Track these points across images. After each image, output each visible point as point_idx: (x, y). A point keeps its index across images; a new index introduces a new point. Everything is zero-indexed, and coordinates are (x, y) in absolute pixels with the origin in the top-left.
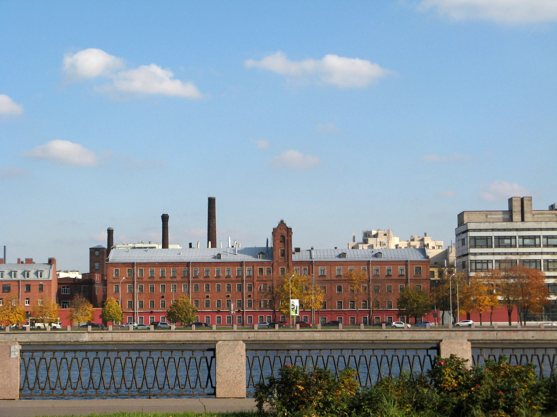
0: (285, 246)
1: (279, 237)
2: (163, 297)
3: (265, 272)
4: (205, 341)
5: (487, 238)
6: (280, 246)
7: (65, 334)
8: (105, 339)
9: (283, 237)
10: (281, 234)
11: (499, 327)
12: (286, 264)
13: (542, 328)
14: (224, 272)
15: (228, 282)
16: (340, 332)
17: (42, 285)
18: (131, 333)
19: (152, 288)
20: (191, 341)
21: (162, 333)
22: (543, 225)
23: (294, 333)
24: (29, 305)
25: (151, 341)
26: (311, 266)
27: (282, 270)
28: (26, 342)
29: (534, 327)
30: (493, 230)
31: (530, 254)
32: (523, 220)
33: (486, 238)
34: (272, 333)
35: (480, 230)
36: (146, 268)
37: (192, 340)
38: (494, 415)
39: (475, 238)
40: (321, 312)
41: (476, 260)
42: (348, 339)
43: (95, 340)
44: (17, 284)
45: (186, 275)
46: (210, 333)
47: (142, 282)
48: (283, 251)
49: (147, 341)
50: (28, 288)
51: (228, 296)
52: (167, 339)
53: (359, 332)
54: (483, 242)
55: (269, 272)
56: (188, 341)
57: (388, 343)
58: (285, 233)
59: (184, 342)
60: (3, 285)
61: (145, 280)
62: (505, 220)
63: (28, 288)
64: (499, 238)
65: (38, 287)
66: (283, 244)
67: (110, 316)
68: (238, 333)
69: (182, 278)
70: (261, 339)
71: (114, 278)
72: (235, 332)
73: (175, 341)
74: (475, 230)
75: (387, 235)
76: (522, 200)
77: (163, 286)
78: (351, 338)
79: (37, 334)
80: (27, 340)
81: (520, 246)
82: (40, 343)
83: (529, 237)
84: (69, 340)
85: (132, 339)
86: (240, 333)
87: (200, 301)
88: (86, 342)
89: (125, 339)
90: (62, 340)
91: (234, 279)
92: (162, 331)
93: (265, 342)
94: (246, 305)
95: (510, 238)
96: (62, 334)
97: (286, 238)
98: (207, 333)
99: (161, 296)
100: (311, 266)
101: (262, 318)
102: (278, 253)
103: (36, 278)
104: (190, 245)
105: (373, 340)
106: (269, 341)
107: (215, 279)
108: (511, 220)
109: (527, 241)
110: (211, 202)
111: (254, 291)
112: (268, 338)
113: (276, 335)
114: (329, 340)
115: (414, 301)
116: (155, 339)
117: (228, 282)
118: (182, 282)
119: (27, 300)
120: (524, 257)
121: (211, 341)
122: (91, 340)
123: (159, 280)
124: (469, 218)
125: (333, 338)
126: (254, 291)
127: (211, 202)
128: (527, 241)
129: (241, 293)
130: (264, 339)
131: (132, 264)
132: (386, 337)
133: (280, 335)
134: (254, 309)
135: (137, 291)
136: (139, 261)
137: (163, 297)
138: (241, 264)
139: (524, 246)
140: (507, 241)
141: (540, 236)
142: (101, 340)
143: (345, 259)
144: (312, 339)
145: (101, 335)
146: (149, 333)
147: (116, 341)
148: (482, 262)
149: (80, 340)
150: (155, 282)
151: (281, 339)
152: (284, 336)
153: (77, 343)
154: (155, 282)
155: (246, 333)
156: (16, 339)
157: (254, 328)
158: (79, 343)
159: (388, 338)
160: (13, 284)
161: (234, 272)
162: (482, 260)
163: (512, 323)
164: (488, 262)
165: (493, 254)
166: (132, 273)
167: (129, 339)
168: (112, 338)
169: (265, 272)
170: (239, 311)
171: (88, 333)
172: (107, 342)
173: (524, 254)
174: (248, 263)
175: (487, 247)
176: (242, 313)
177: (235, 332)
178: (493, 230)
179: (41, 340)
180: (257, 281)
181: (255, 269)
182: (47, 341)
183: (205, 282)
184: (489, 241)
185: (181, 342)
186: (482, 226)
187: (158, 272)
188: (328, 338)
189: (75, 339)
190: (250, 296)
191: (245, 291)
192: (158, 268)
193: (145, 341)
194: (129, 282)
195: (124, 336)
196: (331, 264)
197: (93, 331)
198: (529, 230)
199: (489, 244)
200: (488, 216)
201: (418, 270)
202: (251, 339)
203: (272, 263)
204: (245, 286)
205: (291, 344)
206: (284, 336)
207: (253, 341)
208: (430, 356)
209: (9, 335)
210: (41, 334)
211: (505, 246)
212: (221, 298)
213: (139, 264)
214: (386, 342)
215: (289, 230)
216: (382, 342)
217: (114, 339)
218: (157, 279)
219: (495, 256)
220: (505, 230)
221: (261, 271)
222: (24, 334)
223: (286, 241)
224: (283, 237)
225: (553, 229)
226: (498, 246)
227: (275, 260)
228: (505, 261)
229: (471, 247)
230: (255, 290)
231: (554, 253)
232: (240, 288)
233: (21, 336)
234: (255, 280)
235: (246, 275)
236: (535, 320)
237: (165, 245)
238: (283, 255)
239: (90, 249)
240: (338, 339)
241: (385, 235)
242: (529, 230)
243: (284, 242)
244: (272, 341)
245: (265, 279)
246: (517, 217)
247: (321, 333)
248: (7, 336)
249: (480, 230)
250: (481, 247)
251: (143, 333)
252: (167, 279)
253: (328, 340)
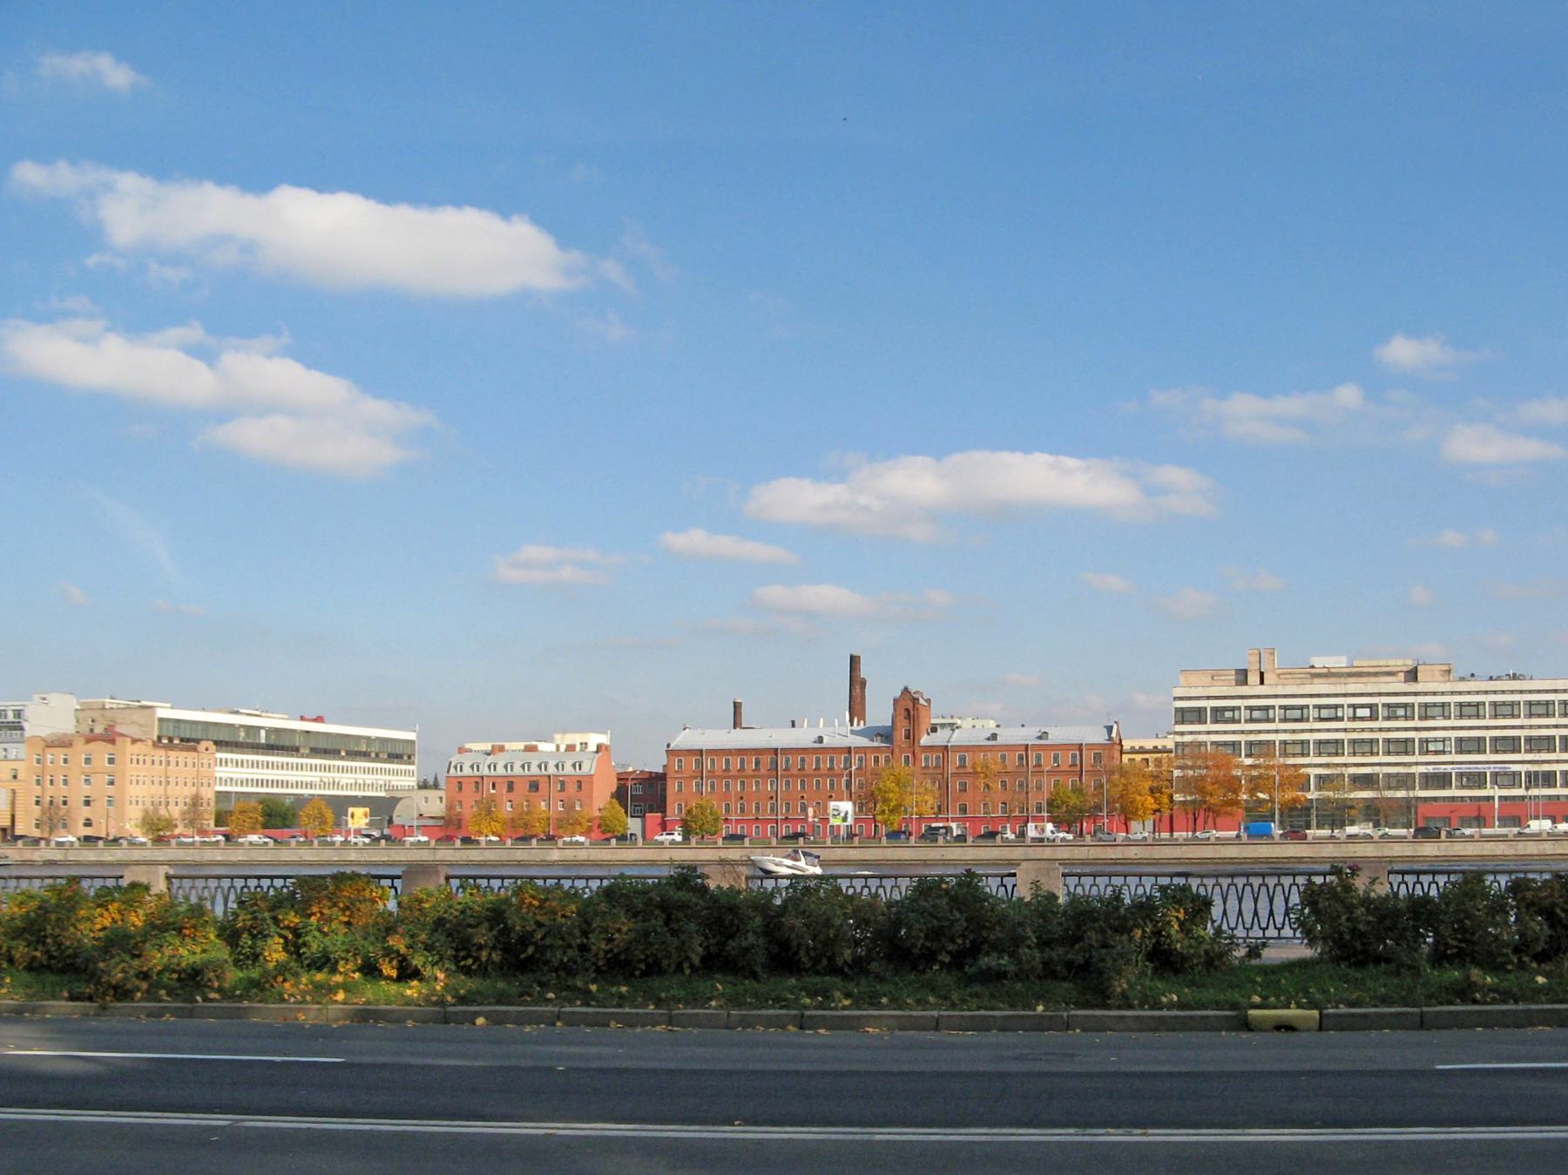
2: (742, 798)
9: (907, 710)
12: (911, 750)
19: (727, 785)
30: (1208, 698)
32: (1262, 682)
35: (1190, 698)
47: (714, 777)
52: (658, 859)
54: (1195, 716)
55: (887, 760)
58: (910, 706)
61: (717, 774)
64: (1215, 710)
77: (743, 783)
78: (896, 858)
81: (1246, 721)
83: (1259, 708)
85: (614, 858)
95: (1233, 709)
97: (912, 713)
102: (900, 734)
104: (793, 722)
107: (812, 772)
108: (1245, 682)
109: (1256, 714)
110: (854, 661)
115: (1063, 802)
128: (1256, 714)
137: (742, 798)
139: (1252, 720)
140: (1228, 714)
144: (846, 858)
165: (1208, 733)
166: (699, 763)
167: (609, 858)
173: (1251, 732)
174: (859, 749)
178: (1208, 698)
186: (1193, 693)
187: (736, 762)
201: (1098, 757)
208: (1251, 885)
211: (1226, 721)
212: (821, 798)
213: (710, 752)
221: (877, 760)
224: (907, 710)
226: (1216, 721)
229: (1176, 723)
238: (908, 737)
249: (1190, 698)
250: (1192, 723)
252: (746, 773)
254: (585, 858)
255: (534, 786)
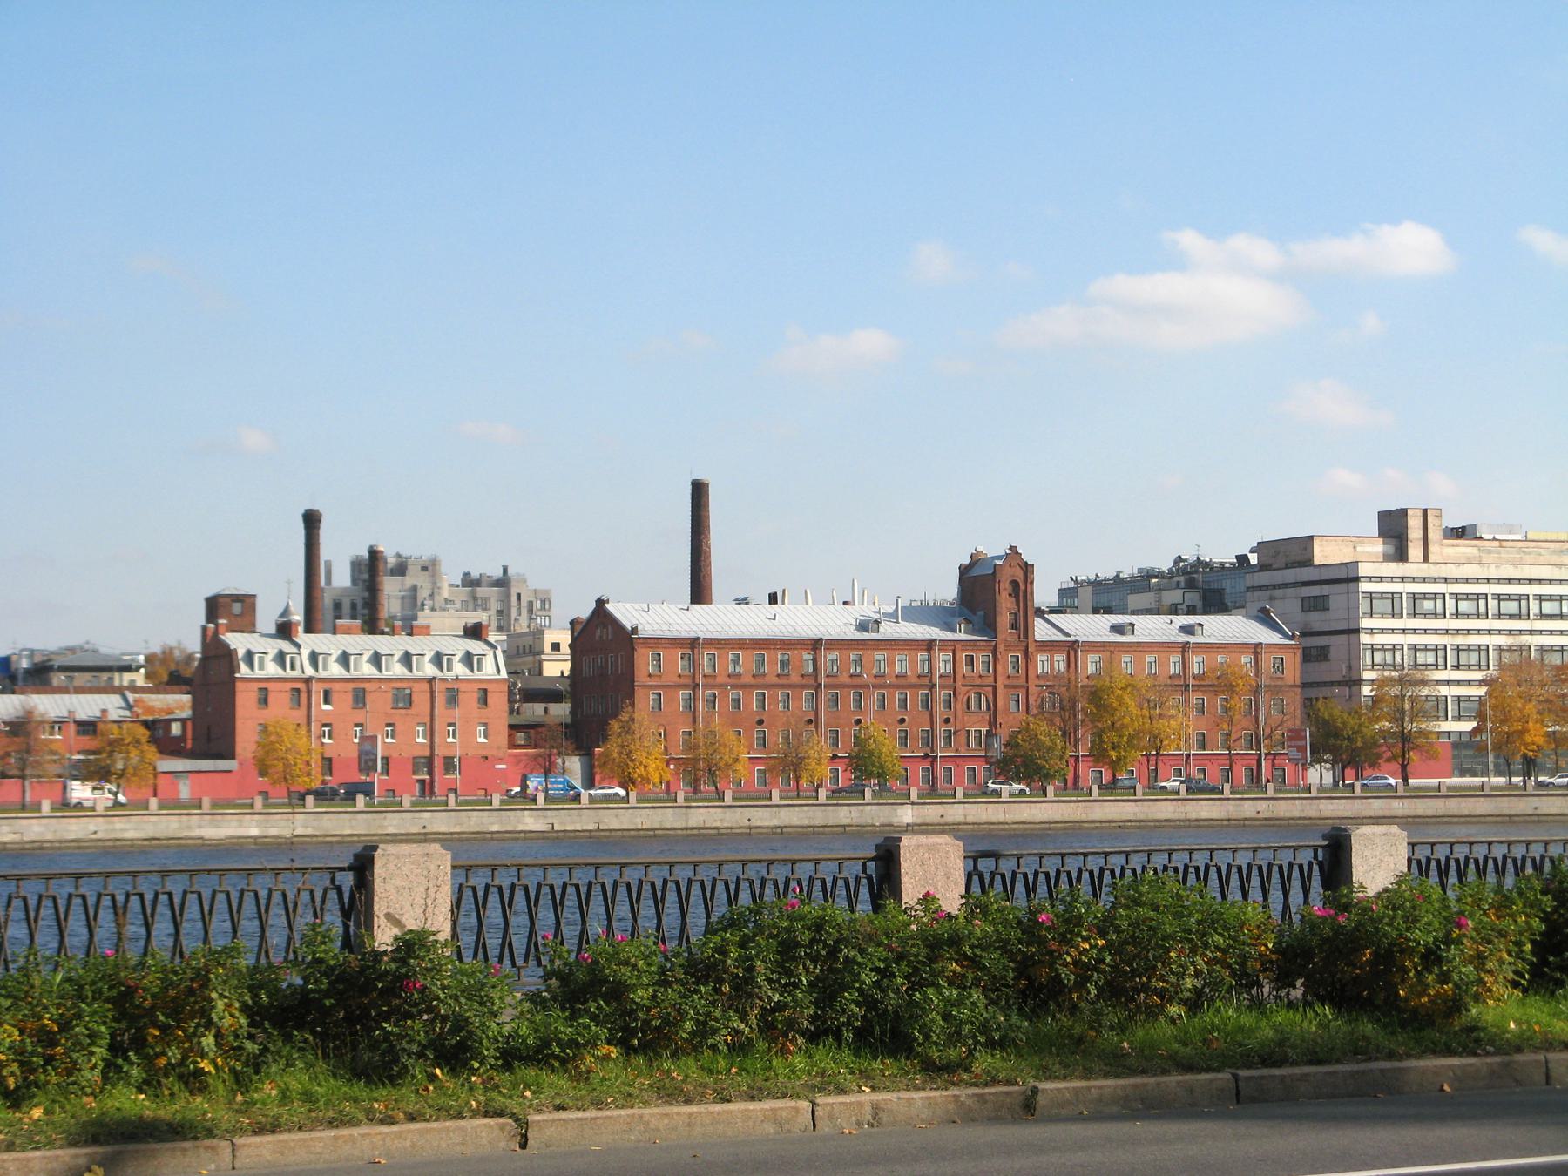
0: (1018, 604)
1: (1007, 585)
2: (761, 722)
3: (979, 667)
4: (1166, 820)
5: (1392, 597)
6: (1009, 606)
7: (861, 808)
8: (949, 819)
10: (1013, 576)
11: (1449, 788)
13: (1444, 792)
14: (892, 663)
15: (903, 687)
16: (1443, 800)
17: (485, 691)
18: (1005, 805)
20: (1135, 821)
21: (1072, 804)
22: (1493, 572)
23: (1349, 801)
24: (454, 740)
25: (1050, 823)
26: (1072, 653)
27: (1014, 660)
28: (772, 828)
29: (1470, 788)
31: (1541, 632)
32: (1426, 559)
33: (1390, 596)
34: (1304, 801)
36: (723, 651)
37: (1138, 818)
38: (1254, 991)
39: (1371, 596)
40: (1085, 759)
41: (1372, 645)
42: (1460, 814)
43: (927, 821)
44: (426, 686)
45: (811, 669)
46: (1174, 803)
48: (1013, 617)
49: (1041, 823)
50: (360, 698)
51: (902, 721)
52: (1084, 817)
53: (1482, 799)
54: (1384, 606)
56: (1130, 821)
57: (1539, 822)
59: (1121, 824)
60: (393, 688)
61: (720, 680)
62: (1387, 558)
63: (360, 698)
64: (1414, 597)
65: (476, 695)
66: (1014, 599)
67: (881, 766)
68: (1233, 802)
69: (803, 676)
70: (1282, 815)
71: (650, 675)
72: (1228, 799)
73: (1101, 822)
74: (1370, 579)
75: (430, 568)
76: (1425, 512)
78: (1466, 812)
79: (797, 808)
80: (775, 822)
82: (805, 830)
83: (1467, 597)
84: (870, 822)
85: (1009, 818)
86: (1239, 802)
87: (843, 732)
88: (908, 825)
89: (994, 819)
90: (855, 822)
91: (914, 681)
92: (560, 806)
93: (1291, 822)
94: (940, 743)
96: (853, 808)
97: (1022, 587)
98: (1169, 803)
99: (757, 719)
100: (1072, 653)
101: (1098, 775)
103: (468, 672)
105: (1510, 816)
106: (1300, 818)
109: (1464, 606)
110: (699, 491)
111: (955, 708)
112: (1296, 814)
113: (1314, 807)
114: (1424, 817)
116: (1058, 817)
117: (903, 687)
118: (804, 687)
119: (389, 729)
120: (1460, 640)
121: (1180, 821)
122: (919, 821)
123: (752, 681)
124: (1322, 551)
125: (1430, 812)
126: (955, 708)
127: (699, 491)
129: (928, 713)
130: (1288, 815)
131: (693, 643)
132: (1536, 808)
133: (1231, 808)
134: (957, 751)
135: (702, 706)
136: (709, 636)
137: (761, 722)
138: (929, 645)
140: (1428, 605)
141: (1486, 595)
142: (942, 821)
143: (1131, 637)
145: (940, 810)
146: (1044, 805)
147: (974, 824)
148: (1383, 648)
149: (895, 821)
150: (743, 686)
151: (1326, 814)
152: (1331, 807)
153: (887, 828)
154: (743, 686)
155: (1250, 802)
156: (749, 820)
157: (770, 799)
158: (892, 828)
159: (1539, 812)
160: (416, 687)
161: (913, 663)
162: (1383, 645)
163: (1410, 781)
164: (1394, 648)
166: (693, 664)
167: (1001, 818)
168: (965, 816)
169: (979, 667)
170: (926, 756)
171: (913, 804)
172: (954, 824)
174: (945, 644)
175: (1478, 616)
176: (930, 760)
177: (1228, 799)
179: (806, 823)
180: (963, 686)
181: (957, 658)
182: (822, 823)
183: (898, 687)
184: (1397, 602)
185: (1114, 824)
187: (749, 659)
188: (1420, 812)
189: (883, 820)
190: (947, 721)
191: (939, 709)
192: (748, 652)
193: (1037, 821)
194: (685, 686)
195: (990, 810)
196: (1112, 649)
197: (1057, 799)
198: (1467, 580)
199: (1397, 610)
200: (1359, 549)
202: (1261, 815)
203: (993, 643)
204: (940, 695)
205: (1427, 824)
206: (1331, 807)
207: (1265, 819)
209: (732, 810)
210: (806, 808)
211: (1425, 616)
213: (710, 642)
214: (1536, 818)
215: (1027, 569)
216: (1527, 818)
217: (970, 819)
218: (747, 680)
219: (1534, 637)
220: (1424, 580)
222: (768, 809)
223: (1021, 594)
224: (1015, 584)
225: (1561, 582)
227: (1001, 636)
228: (1510, 649)
230: (959, 706)
231: (1562, 632)
232: (928, 704)
233: (760, 813)
234: (959, 684)
235: (825, 671)
236: (1474, 775)
237: (699, 592)
238: (1014, 626)
239: (770, 604)
240: (1440, 813)
241: (425, 569)
242: (1467, 580)
243: (1017, 597)
244: (1305, 818)
245: (978, 682)
246: (1414, 551)
247: (1406, 801)
248: (729, 812)
251: (1032, 805)
253: (1419, 817)
254: (960, 819)
255: (403, 699)
